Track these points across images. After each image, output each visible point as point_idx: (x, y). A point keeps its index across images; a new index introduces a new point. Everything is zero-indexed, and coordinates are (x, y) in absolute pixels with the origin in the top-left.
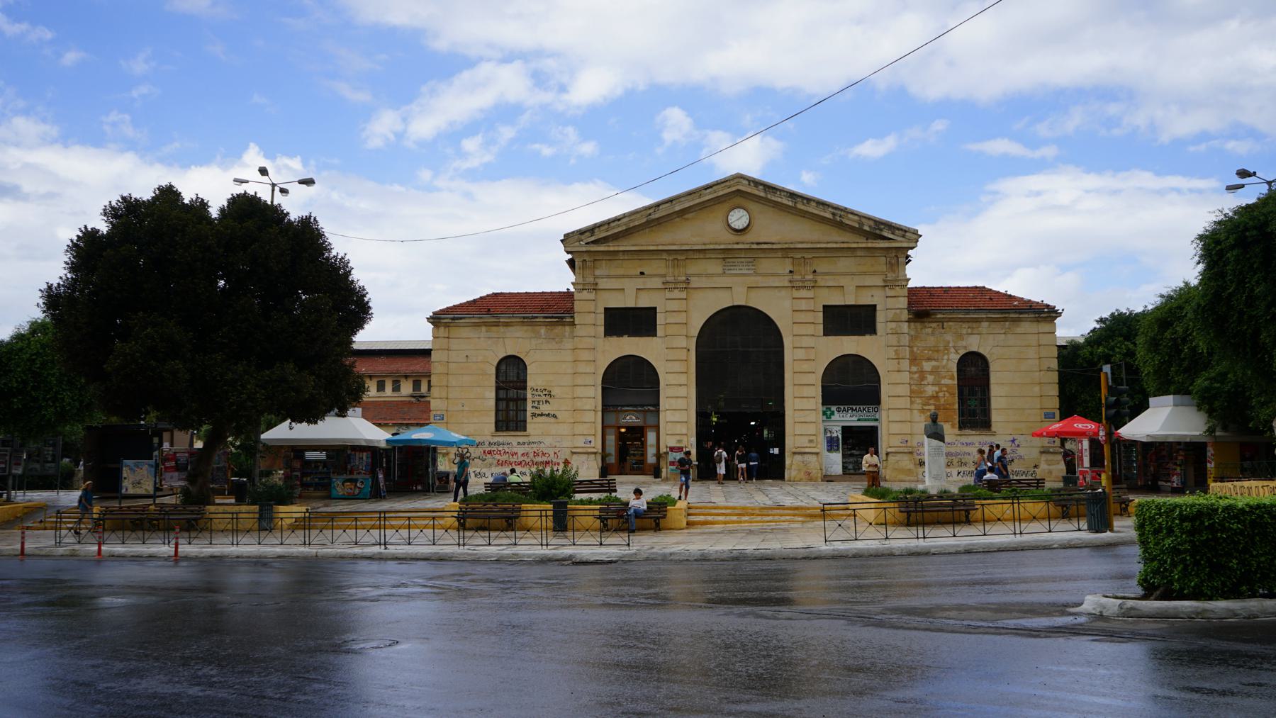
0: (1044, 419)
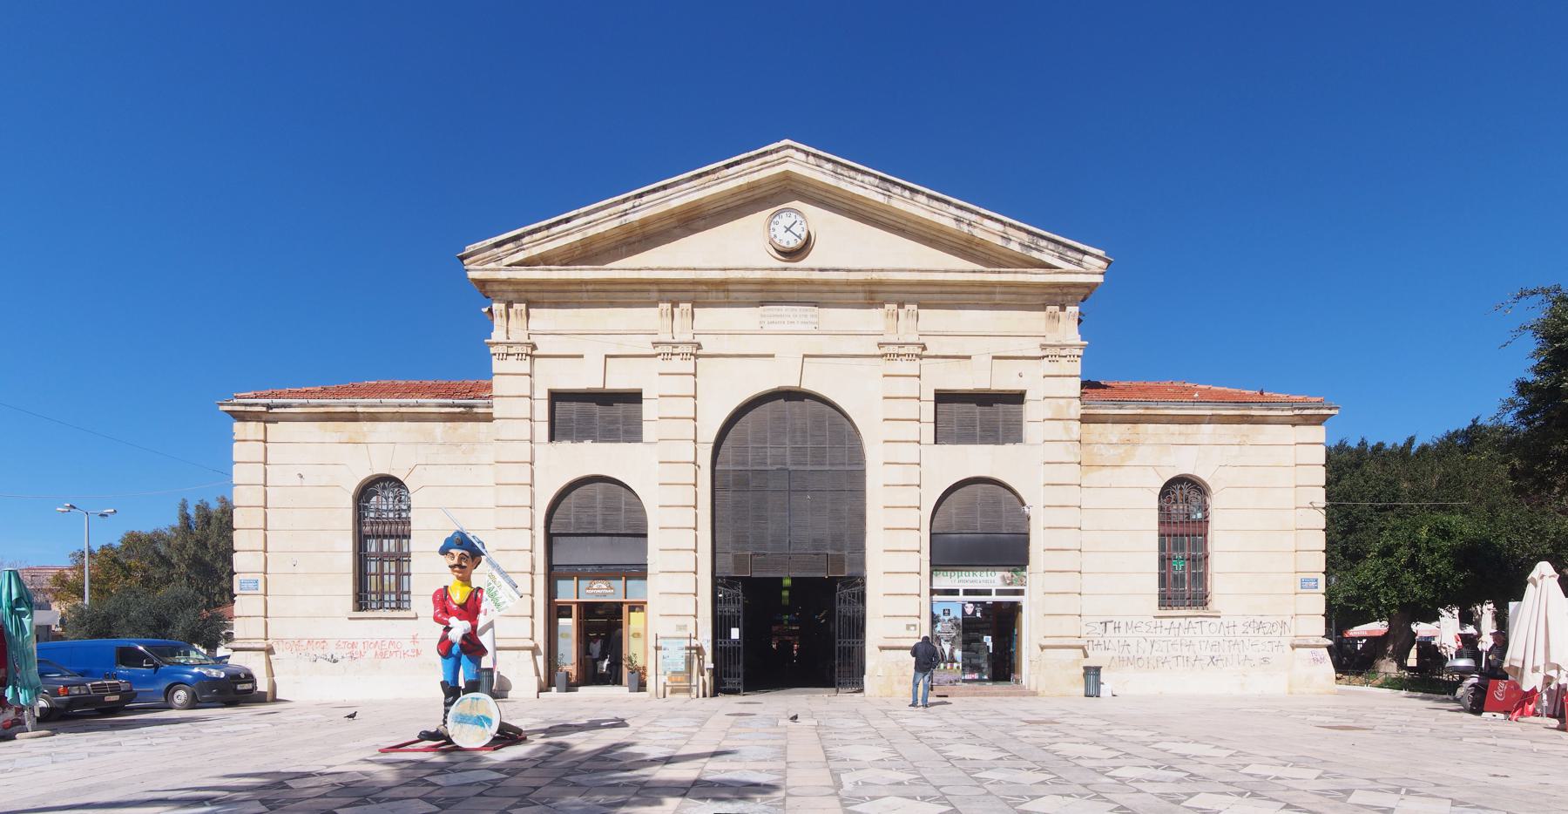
0: (1299, 590)
